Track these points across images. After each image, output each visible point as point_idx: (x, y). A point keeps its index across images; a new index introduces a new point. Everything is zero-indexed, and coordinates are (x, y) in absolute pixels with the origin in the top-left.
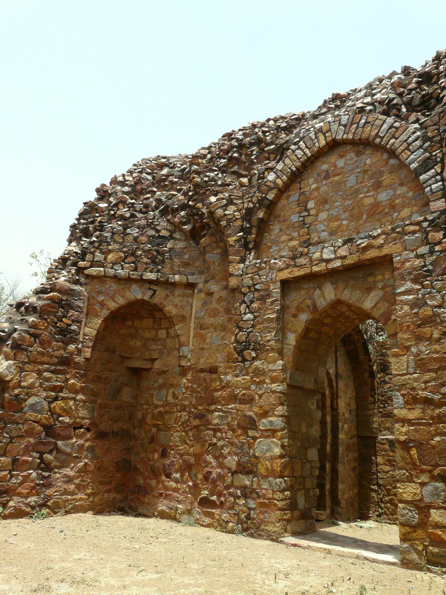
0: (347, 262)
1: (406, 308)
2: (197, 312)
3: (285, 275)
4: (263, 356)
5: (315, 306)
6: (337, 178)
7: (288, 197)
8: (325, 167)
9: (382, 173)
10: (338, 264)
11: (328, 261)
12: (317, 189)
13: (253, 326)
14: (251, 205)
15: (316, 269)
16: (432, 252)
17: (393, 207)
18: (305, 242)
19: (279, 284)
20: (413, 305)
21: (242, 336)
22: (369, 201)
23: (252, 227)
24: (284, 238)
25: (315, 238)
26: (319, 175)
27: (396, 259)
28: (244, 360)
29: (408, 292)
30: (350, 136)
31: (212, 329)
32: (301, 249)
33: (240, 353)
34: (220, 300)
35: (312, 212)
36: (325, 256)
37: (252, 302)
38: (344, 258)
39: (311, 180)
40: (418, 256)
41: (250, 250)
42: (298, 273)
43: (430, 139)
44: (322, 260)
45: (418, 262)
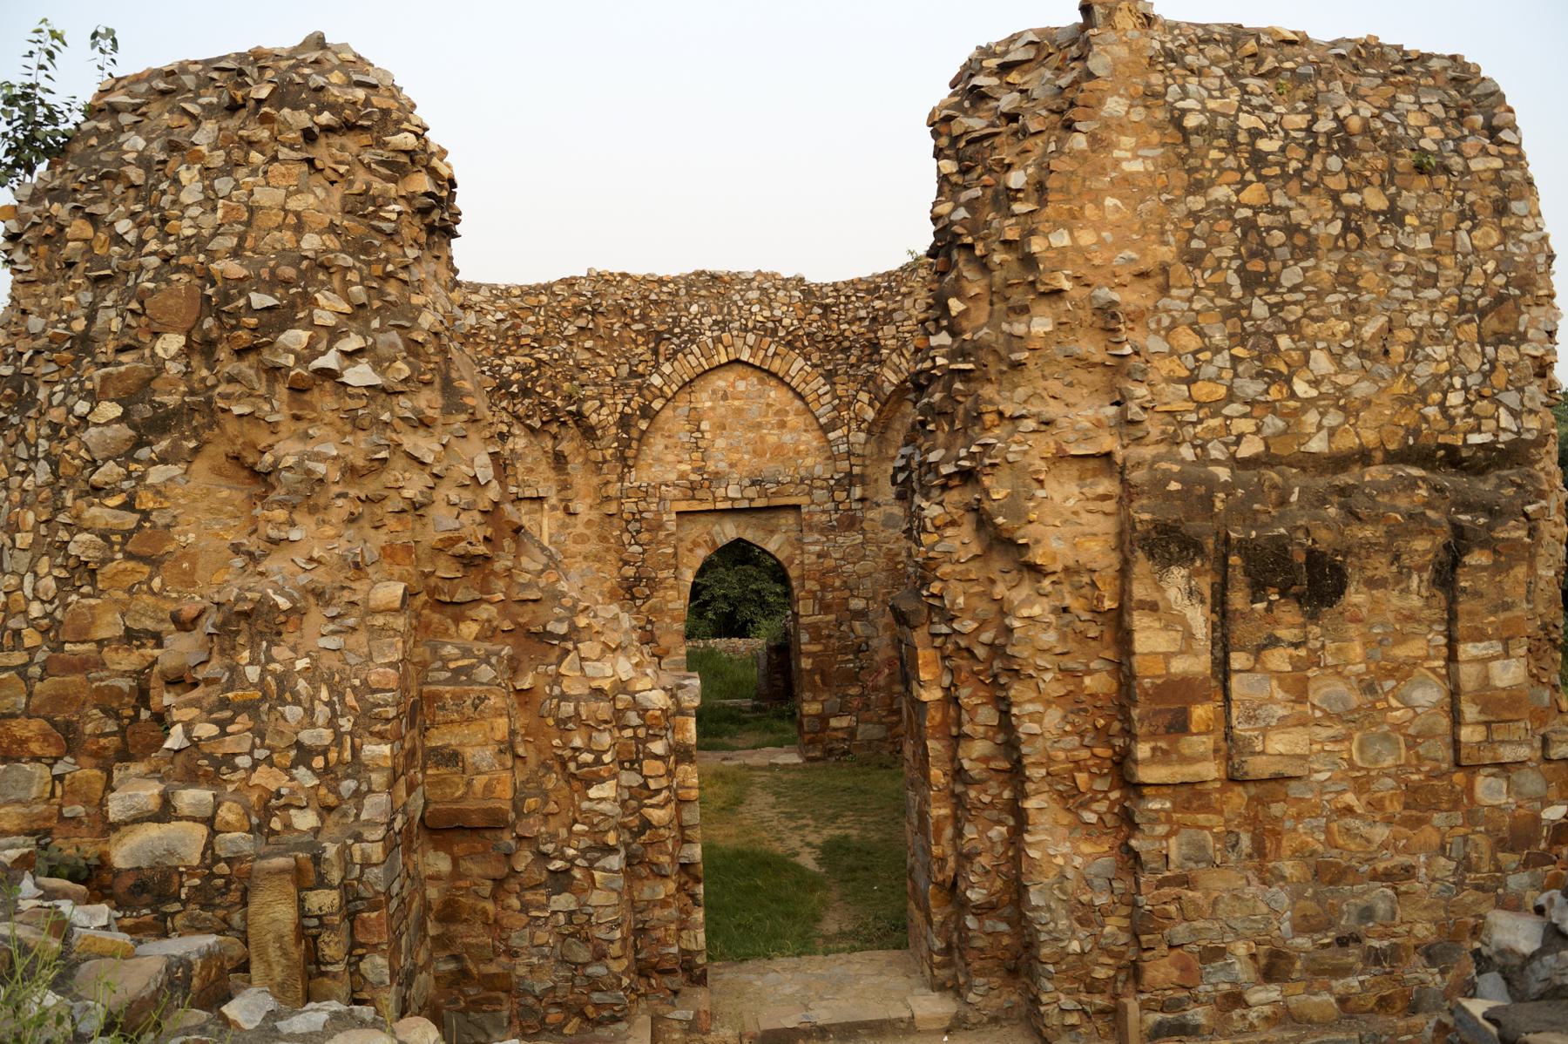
0: (754, 505)
1: (814, 558)
2: (551, 536)
3: (683, 506)
4: (661, 593)
5: (714, 542)
6: (737, 403)
7: (675, 409)
8: (721, 384)
9: (787, 412)
10: (745, 504)
11: (733, 500)
12: (712, 409)
13: (643, 561)
14: (628, 410)
15: (720, 506)
16: (837, 510)
17: (798, 453)
18: (700, 469)
19: (674, 516)
20: (819, 556)
21: (630, 571)
22: (772, 439)
23: (630, 439)
24: (670, 457)
25: (711, 467)
26: (714, 392)
27: (804, 510)
28: (633, 598)
29: (815, 543)
30: (757, 363)
31: (580, 558)
32: (693, 477)
33: (629, 589)
34: (589, 523)
35: (707, 435)
36: (731, 494)
37: (638, 532)
38: (752, 500)
39: (704, 396)
40: (824, 512)
41: (630, 467)
42: (696, 506)
43: (840, 398)
44: (726, 498)
45: (824, 518)
